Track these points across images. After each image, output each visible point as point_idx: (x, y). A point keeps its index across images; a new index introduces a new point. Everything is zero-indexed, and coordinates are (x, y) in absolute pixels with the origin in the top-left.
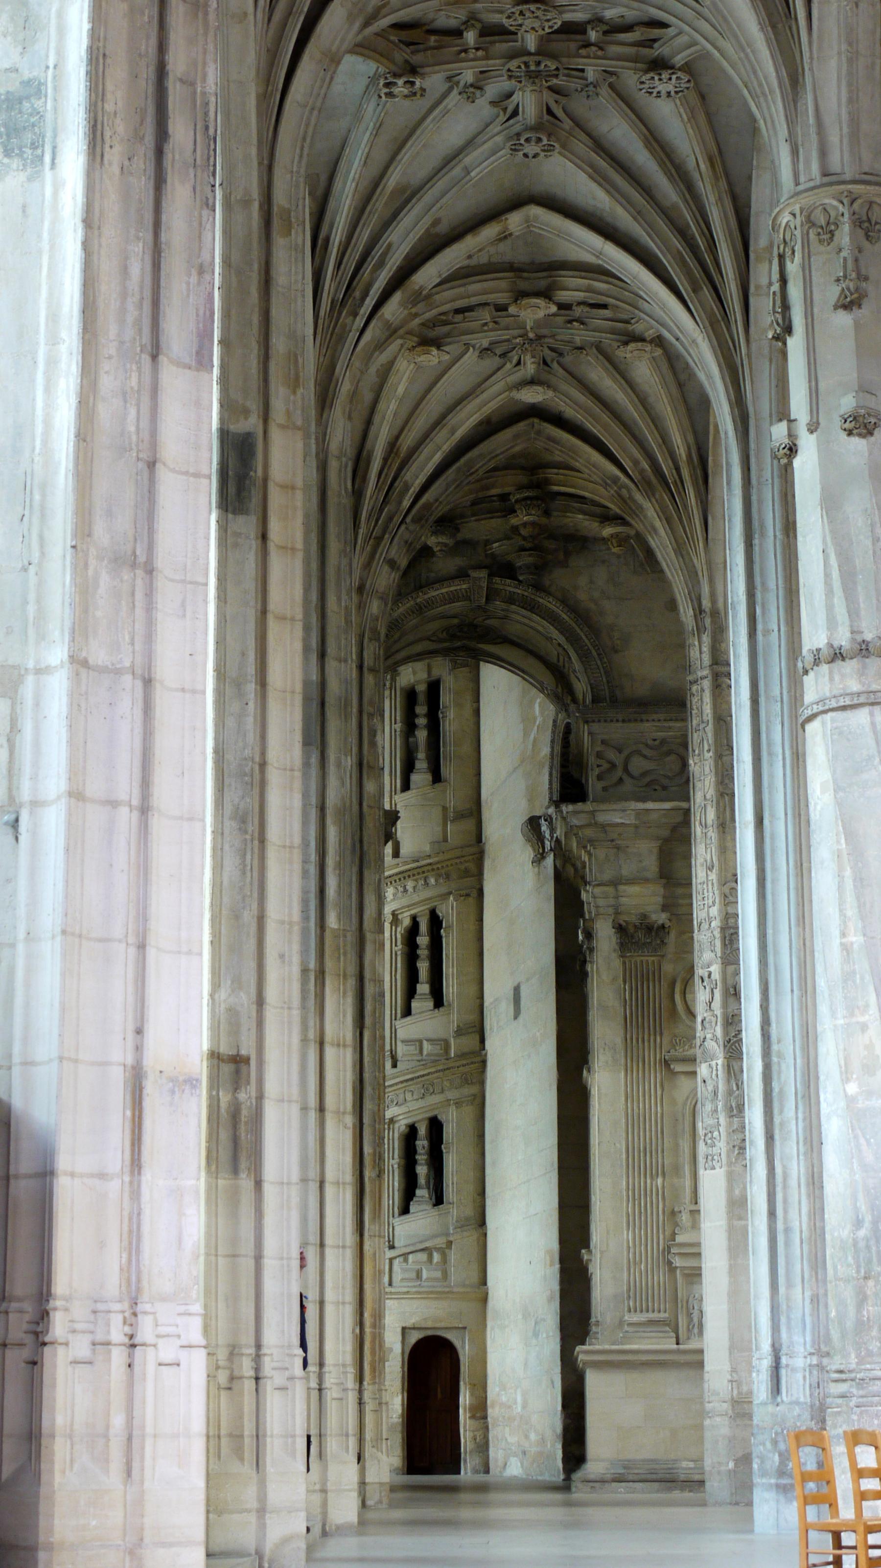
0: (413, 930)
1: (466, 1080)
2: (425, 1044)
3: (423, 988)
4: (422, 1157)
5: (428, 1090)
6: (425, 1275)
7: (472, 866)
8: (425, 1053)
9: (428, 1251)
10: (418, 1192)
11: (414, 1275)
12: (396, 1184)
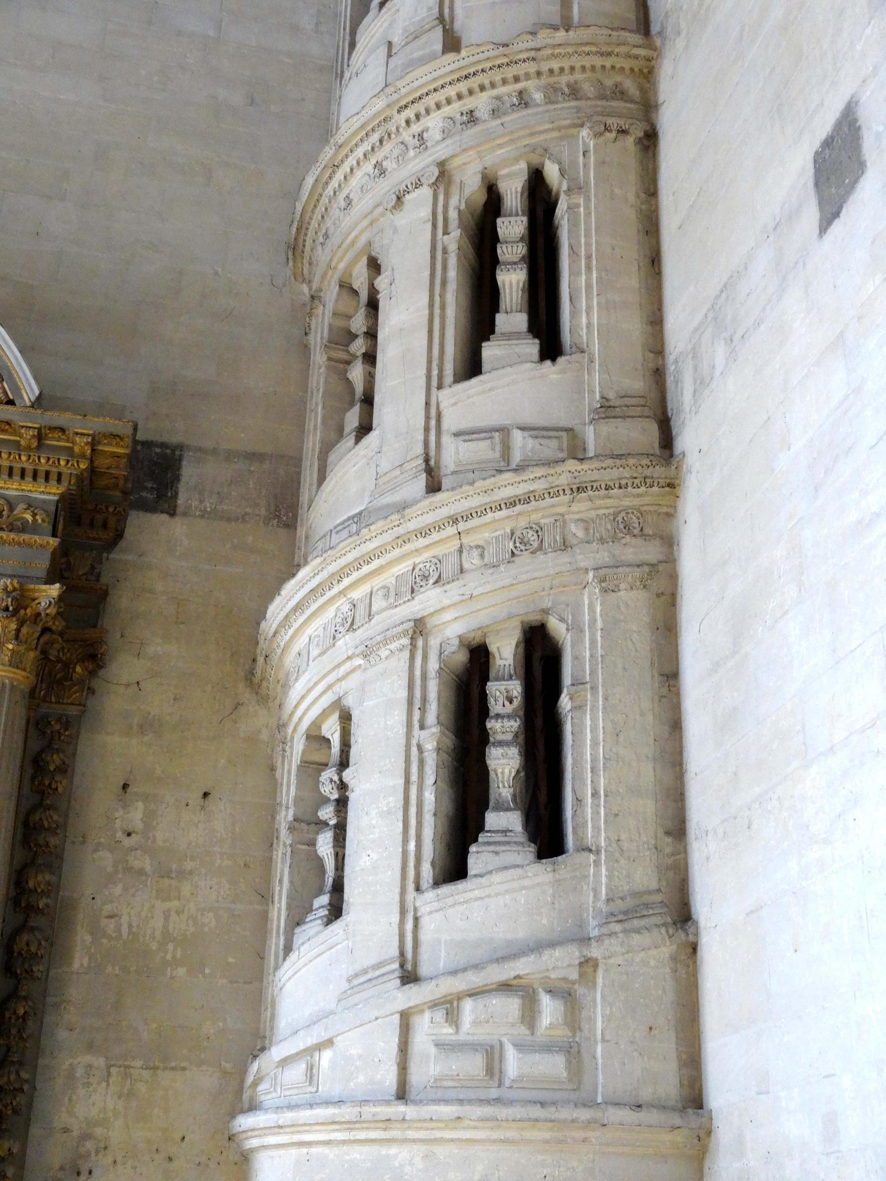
0: (493, 204)
1: (627, 527)
2: (518, 437)
3: (512, 318)
4: (504, 724)
5: (521, 545)
6: (513, 1064)
7: (630, 86)
8: (517, 457)
9: (523, 991)
10: (492, 819)
11: (475, 1064)
12: (430, 797)
